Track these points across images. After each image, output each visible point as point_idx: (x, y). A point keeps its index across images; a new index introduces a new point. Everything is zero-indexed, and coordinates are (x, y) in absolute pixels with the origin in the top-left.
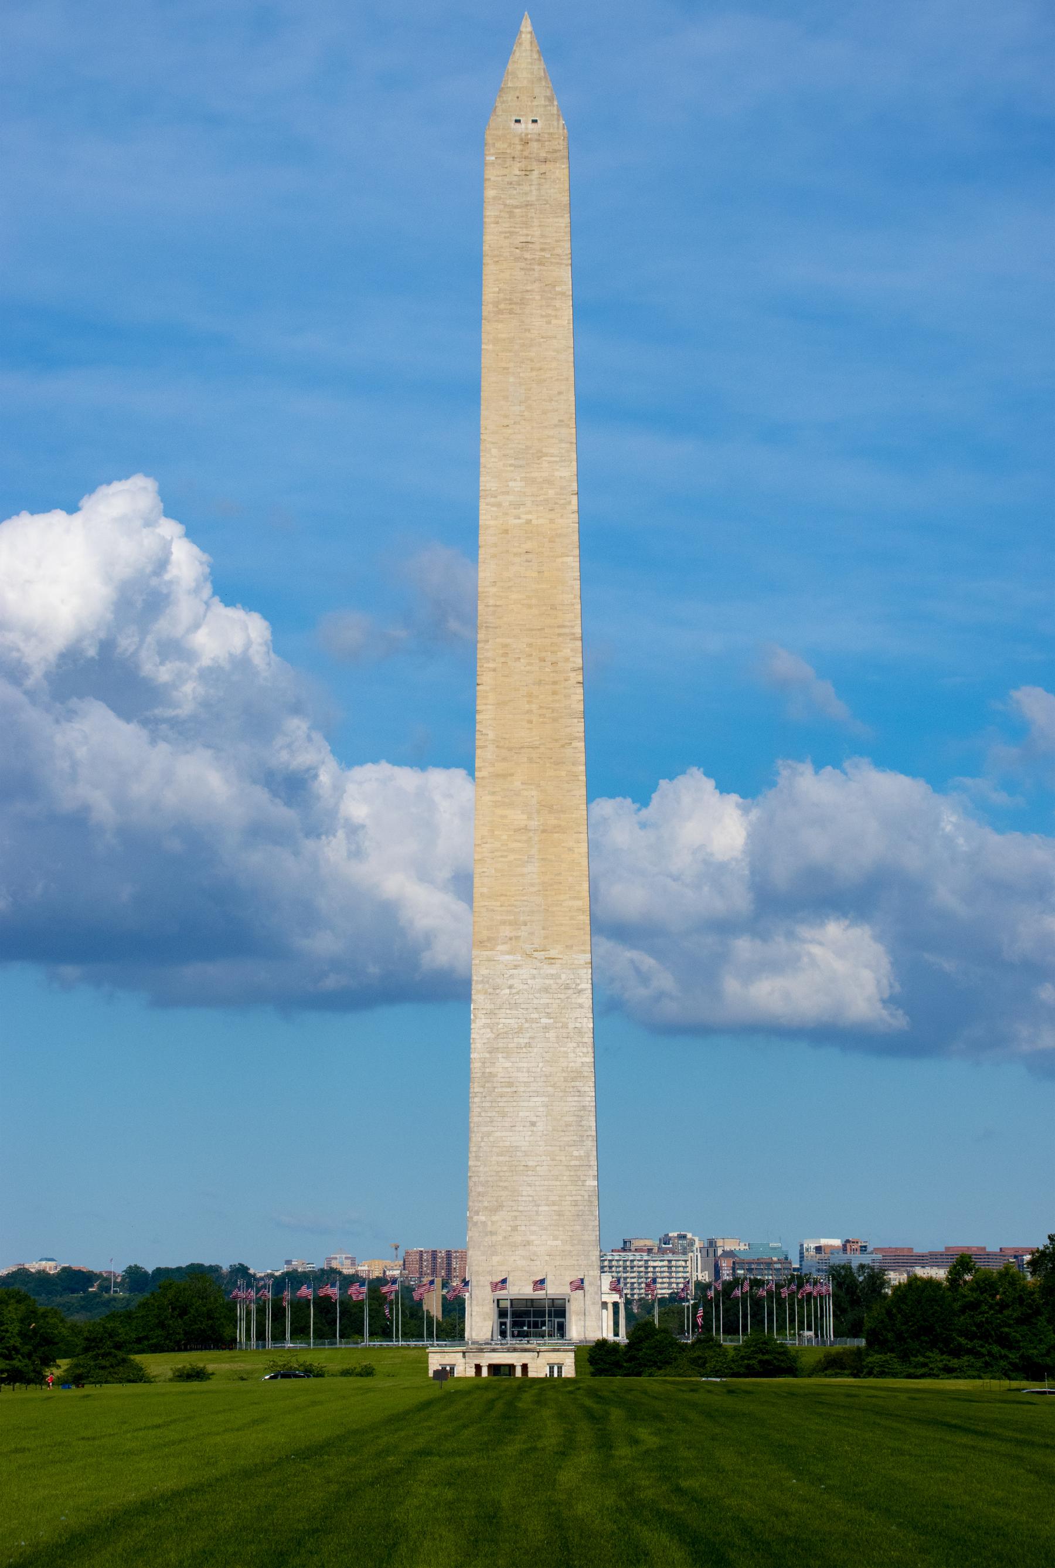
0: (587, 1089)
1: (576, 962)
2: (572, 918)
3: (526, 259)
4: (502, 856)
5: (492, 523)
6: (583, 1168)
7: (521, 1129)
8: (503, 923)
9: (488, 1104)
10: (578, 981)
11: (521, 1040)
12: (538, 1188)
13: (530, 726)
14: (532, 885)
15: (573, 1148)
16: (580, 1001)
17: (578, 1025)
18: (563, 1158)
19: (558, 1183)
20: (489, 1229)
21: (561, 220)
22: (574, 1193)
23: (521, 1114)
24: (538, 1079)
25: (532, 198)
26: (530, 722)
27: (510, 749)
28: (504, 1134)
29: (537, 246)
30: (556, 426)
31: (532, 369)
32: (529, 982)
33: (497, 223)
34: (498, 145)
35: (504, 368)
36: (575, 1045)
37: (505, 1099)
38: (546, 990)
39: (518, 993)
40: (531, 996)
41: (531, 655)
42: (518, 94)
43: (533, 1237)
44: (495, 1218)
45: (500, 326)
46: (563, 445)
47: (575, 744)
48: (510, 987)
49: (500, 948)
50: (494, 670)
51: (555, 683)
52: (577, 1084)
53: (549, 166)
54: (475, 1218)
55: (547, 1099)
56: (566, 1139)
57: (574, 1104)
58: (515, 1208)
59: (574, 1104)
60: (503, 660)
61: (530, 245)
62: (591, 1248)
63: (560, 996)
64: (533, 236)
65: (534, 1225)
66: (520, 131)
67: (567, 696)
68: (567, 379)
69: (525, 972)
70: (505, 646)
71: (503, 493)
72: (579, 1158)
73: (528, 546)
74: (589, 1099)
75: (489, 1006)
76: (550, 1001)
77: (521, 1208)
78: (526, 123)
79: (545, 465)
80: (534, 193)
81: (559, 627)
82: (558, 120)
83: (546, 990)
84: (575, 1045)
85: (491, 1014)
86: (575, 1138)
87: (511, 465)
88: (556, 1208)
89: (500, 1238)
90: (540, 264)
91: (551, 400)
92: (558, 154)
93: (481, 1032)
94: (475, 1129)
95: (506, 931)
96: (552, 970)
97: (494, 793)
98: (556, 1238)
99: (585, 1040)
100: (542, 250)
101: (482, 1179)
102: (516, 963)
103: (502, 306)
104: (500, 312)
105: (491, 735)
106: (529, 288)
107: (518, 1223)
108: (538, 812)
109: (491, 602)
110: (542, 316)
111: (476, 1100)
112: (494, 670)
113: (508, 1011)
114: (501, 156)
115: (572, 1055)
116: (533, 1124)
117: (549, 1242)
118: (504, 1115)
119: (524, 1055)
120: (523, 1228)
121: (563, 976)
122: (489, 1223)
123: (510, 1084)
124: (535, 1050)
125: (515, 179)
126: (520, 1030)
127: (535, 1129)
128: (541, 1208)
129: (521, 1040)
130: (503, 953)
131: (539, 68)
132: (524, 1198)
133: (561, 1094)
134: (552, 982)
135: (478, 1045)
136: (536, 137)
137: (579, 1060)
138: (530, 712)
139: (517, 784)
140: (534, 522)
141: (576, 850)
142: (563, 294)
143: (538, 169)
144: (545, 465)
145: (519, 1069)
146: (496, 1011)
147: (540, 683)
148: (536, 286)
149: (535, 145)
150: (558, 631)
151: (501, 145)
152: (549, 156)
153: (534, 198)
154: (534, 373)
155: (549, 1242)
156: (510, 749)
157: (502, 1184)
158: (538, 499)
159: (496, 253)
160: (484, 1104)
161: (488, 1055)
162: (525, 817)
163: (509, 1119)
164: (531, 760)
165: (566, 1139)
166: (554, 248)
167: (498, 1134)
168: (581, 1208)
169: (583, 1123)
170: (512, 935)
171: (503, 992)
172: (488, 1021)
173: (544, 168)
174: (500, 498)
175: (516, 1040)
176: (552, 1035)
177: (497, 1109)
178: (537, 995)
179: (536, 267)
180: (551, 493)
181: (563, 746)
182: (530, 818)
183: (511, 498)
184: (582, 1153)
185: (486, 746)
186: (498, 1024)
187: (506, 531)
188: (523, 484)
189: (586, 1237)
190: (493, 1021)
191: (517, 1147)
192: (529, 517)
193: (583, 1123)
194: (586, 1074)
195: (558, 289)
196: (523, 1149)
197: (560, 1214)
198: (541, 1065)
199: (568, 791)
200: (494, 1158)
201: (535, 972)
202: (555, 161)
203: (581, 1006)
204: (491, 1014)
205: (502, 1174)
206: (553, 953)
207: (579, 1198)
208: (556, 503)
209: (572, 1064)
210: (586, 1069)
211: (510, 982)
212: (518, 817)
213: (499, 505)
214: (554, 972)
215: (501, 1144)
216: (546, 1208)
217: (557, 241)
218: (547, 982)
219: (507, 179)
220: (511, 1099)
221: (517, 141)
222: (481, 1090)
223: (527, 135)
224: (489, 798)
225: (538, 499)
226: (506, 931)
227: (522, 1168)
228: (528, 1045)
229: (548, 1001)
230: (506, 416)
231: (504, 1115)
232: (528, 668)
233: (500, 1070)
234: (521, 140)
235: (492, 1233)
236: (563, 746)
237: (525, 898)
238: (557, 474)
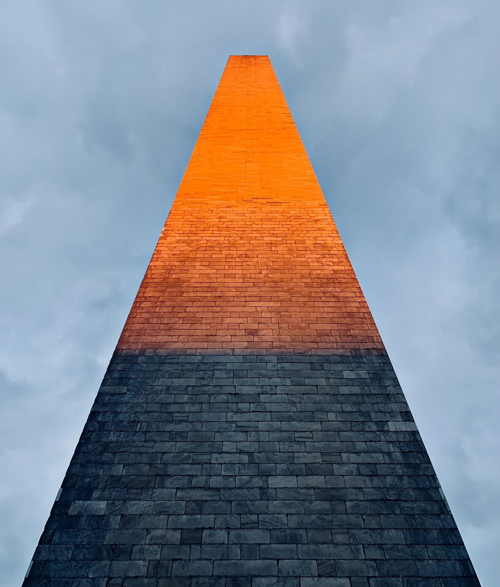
12: (264, 437)
19: (318, 426)
20: (109, 538)
58: (200, 481)
65: (254, 525)
77: (214, 482)
88: (318, 481)
107: (206, 519)
120: (221, 536)
122: (115, 522)
132: (227, 458)
157: (171, 427)
163: (204, 327)
168: (389, 480)
196: (229, 366)
207: (380, 457)
216: (291, 482)
235: (117, 552)
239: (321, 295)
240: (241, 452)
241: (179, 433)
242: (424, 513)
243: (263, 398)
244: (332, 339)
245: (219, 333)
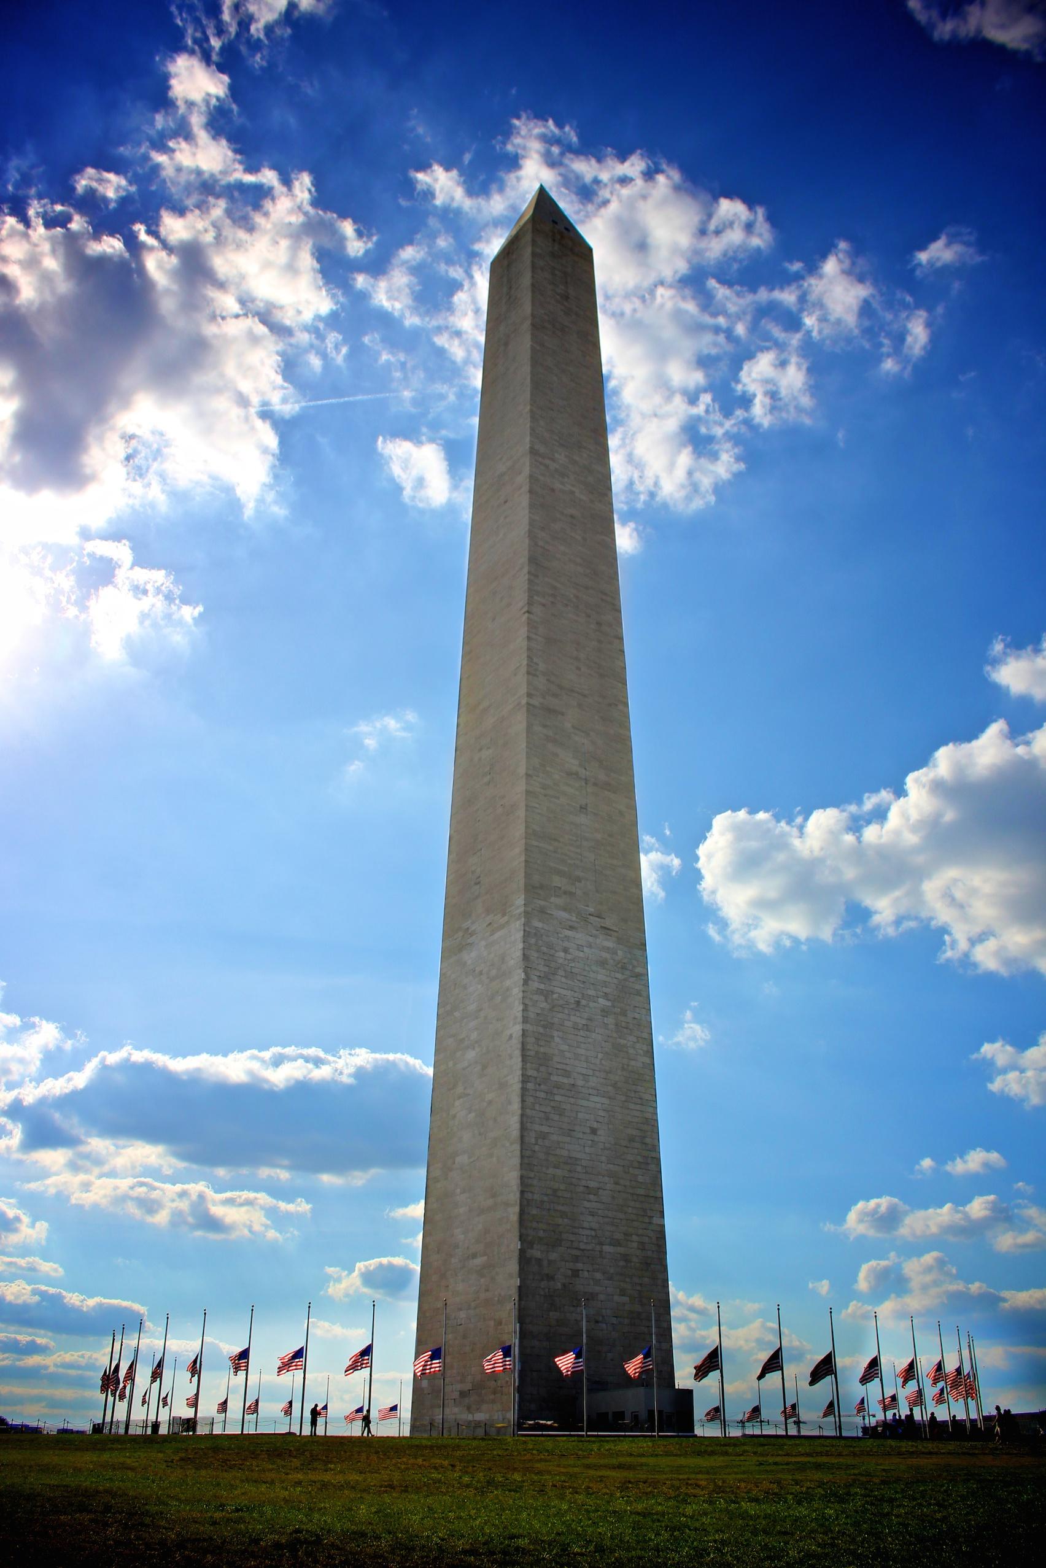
9: (543, 1095)
10: (635, 963)
11: (578, 1020)
15: (637, 1172)
16: (637, 987)
17: (637, 1016)
22: (640, 1232)
26: (579, 669)
32: (585, 949)
37: (562, 1092)
38: (603, 963)
39: (573, 960)
43: (597, 1289)
44: (553, 1256)
49: (553, 899)
55: (606, 1101)
69: (581, 937)
76: (608, 979)
77: (582, 1246)
83: (603, 963)
86: (639, 1158)
89: (559, 1286)
93: (536, 997)
97: (545, 726)
98: (623, 1293)
101: (536, 1197)
107: (580, 1266)
112: (544, 605)
113: (563, 980)
116: (594, 1131)
121: (620, 953)
122: (545, 1263)
124: (594, 1035)
127: (596, 1138)
129: (578, 1020)
133: (623, 1098)
139: (568, 725)
160: (538, 1094)
161: (541, 1030)
162: (577, 762)
168: (649, 1253)
171: (557, 954)
174: (547, 462)
175: (573, 1018)
176: (610, 1020)
177: (552, 1104)
178: (594, 968)
191: (577, 1159)
192: (574, 489)
193: (648, 1140)
196: (584, 1163)
200: (551, 1171)
201: (591, 939)
205: (560, 1193)
206: (608, 923)
209: (633, 1063)
211: (566, 944)
215: (558, 1152)
222: (535, 1073)
226: (557, 881)
227: (581, 1189)
228: (587, 1028)
236: (610, 705)
239: (633, 1095)
240: (591, 1229)
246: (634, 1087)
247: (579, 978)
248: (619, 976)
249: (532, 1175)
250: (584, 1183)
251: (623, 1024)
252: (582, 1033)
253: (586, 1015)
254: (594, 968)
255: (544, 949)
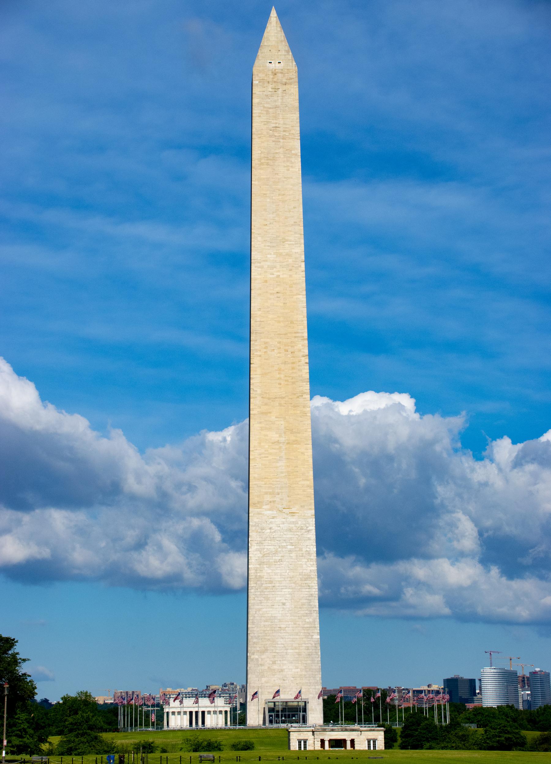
0: (314, 585)
1: (306, 515)
2: (304, 491)
3: (276, 136)
4: (265, 457)
5: (258, 277)
6: (312, 629)
7: (277, 607)
8: (266, 493)
9: (259, 593)
10: (308, 525)
11: (277, 558)
13: (280, 386)
14: (282, 473)
15: (306, 618)
16: (309, 536)
17: (308, 549)
18: (301, 623)
19: (298, 637)
20: (260, 663)
21: (295, 115)
22: (307, 642)
23: (277, 599)
24: (286, 579)
25: (279, 103)
26: (280, 384)
27: (269, 399)
28: (267, 610)
29: (281, 129)
30: (292, 225)
31: (279, 195)
32: (281, 525)
33: (260, 116)
34: (260, 75)
35: (264, 194)
36: (306, 560)
37: (268, 590)
38: (290, 530)
40: (282, 534)
41: (280, 348)
42: (270, 49)
43: (284, 667)
44: (263, 657)
45: (262, 171)
46: (297, 235)
47: (305, 396)
48: (270, 529)
50: (260, 356)
51: (293, 363)
52: (308, 582)
53: (287, 87)
54: (252, 657)
56: (302, 612)
57: (306, 593)
59: (306, 593)
60: (265, 350)
61: (278, 129)
62: (317, 673)
63: (297, 533)
64: (279, 124)
66: (271, 68)
67: (300, 370)
68: (298, 200)
70: (266, 343)
71: (264, 261)
72: (309, 623)
73: (278, 289)
74: (314, 590)
75: (259, 539)
77: (277, 651)
78: (275, 64)
79: (287, 246)
80: (280, 101)
81: (295, 333)
82: (292, 62)
84: (306, 560)
85: (260, 543)
87: (268, 246)
88: (297, 651)
89: (266, 668)
90: (283, 139)
91: (290, 211)
92: (292, 80)
93: (255, 553)
94: (252, 607)
95: (268, 498)
96: (293, 519)
97: (260, 423)
99: (312, 557)
100: (284, 131)
101: (255, 635)
102: (273, 515)
103: (263, 161)
104: (262, 164)
105: (259, 391)
106: (277, 151)
107: (276, 659)
108: (285, 433)
109: (258, 319)
110: (284, 167)
111: (252, 591)
112: (260, 356)
113: (269, 542)
114: (262, 81)
115: (305, 566)
116: (284, 604)
117: (293, 670)
118: (268, 599)
119: (278, 566)
121: (300, 523)
122: (260, 659)
123: (271, 582)
125: (270, 93)
126: (276, 552)
127: (285, 607)
128: (289, 651)
129: (277, 558)
130: (266, 510)
131: (281, 35)
132: (279, 646)
134: (293, 526)
135: (253, 561)
136: (280, 71)
137: (309, 569)
138: (279, 379)
140: (281, 276)
141: (306, 454)
142: (296, 155)
143: (282, 88)
144: (287, 246)
145: (276, 574)
146: (263, 542)
147: (285, 363)
148: (281, 150)
149: (279, 75)
150: (294, 335)
151: (262, 75)
152: (288, 81)
153: (279, 104)
154: (280, 197)
155: (293, 670)
156: (269, 399)
157: (266, 637)
158: (283, 264)
159: (259, 132)
161: (258, 566)
162: (278, 435)
163: (270, 602)
164: (280, 405)
165: (302, 612)
166: (290, 130)
167: (265, 610)
168: (311, 651)
169: (311, 603)
170: (271, 500)
172: (259, 547)
173: (285, 87)
174: (263, 264)
175: (274, 558)
176: (293, 555)
178: (285, 533)
179: (281, 140)
180: (290, 261)
181: (298, 397)
182: (280, 436)
183: (268, 263)
184: (311, 620)
185: (256, 397)
186: (264, 549)
187: (266, 281)
188: (275, 256)
189: (313, 667)
190: (262, 547)
192: (278, 274)
193: (311, 603)
194: (313, 576)
195: (293, 152)
196: (278, 618)
197: (299, 654)
198: (288, 571)
199: (301, 422)
200: (263, 623)
201: (284, 520)
202: (291, 84)
203: (309, 539)
204: (260, 543)
205: (267, 632)
206: (293, 510)
207: (310, 645)
208: (293, 267)
209: (305, 571)
210: (313, 573)
211: (271, 526)
212: (274, 436)
213: (262, 267)
214: (294, 520)
215: (266, 615)
216: (292, 651)
217: (292, 127)
218: (291, 525)
219: (265, 93)
220: (272, 590)
221: (270, 73)
222: (255, 585)
223: (275, 70)
224: (258, 425)
225: (283, 264)
226: (268, 498)
227: (278, 628)
228: (280, 560)
229: (291, 536)
230: (265, 220)
231: (268, 599)
232: (278, 355)
233: (266, 574)
234: (272, 73)
236: (298, 397)
237: (278, 480)
238: (293, 251)
241: (269, 639)
242: (315, 657)
243: (287, 629)
244: (305, 606)
245: (275, 604)
246: (305, 582)
247: (277, 539)
248: (299, 533)
249: (254, 626)
250: (279, 626)
251: (300, 555)
252: (278, 563)
253: (281, 555)
254: (285, 533)
255: (260, 530)
